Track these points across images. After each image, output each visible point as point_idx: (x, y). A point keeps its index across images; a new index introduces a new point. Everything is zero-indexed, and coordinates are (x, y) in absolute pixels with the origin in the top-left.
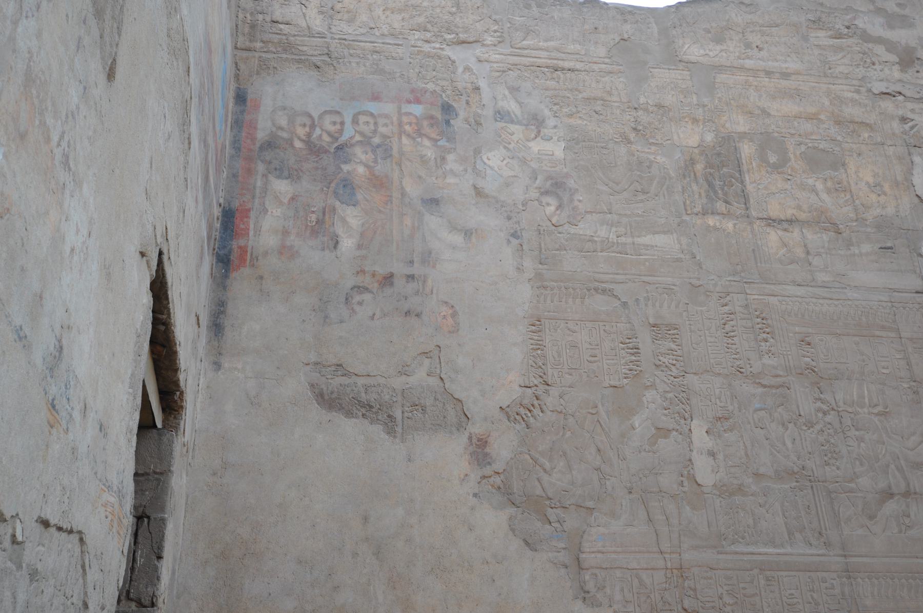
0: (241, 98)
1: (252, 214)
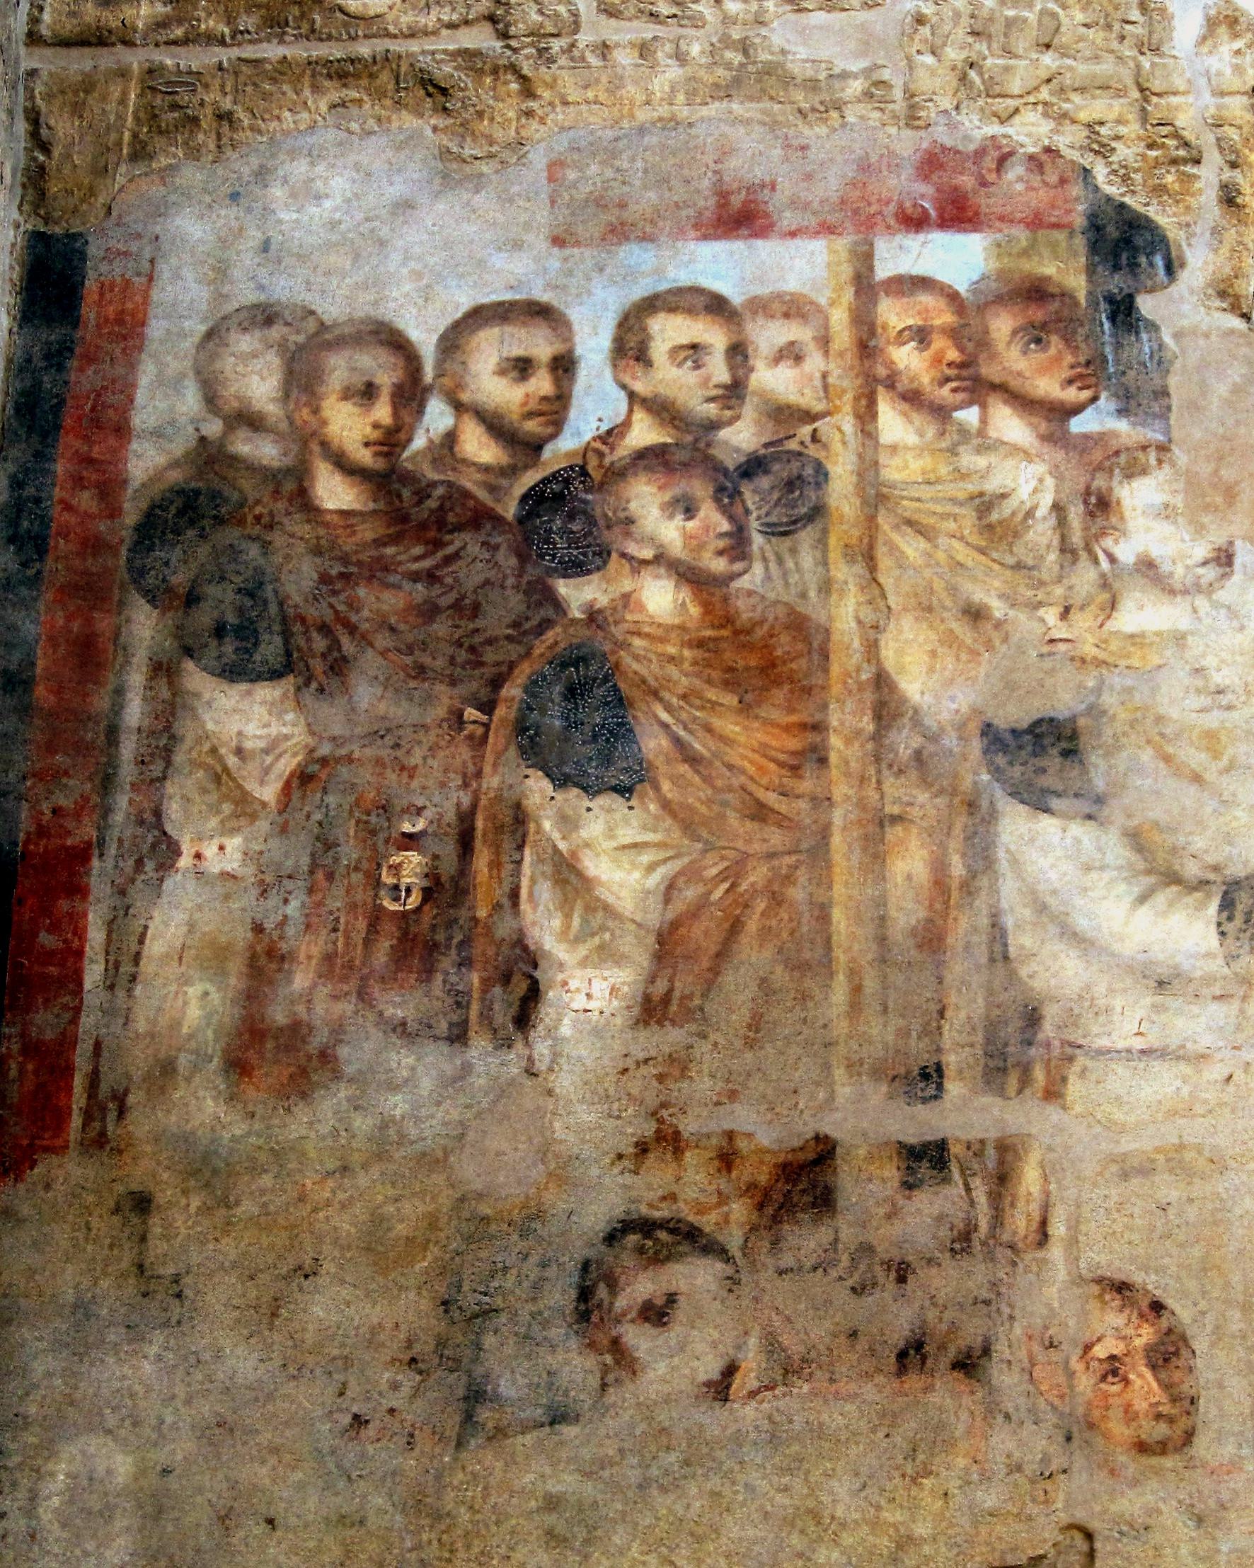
1: (100, 875)
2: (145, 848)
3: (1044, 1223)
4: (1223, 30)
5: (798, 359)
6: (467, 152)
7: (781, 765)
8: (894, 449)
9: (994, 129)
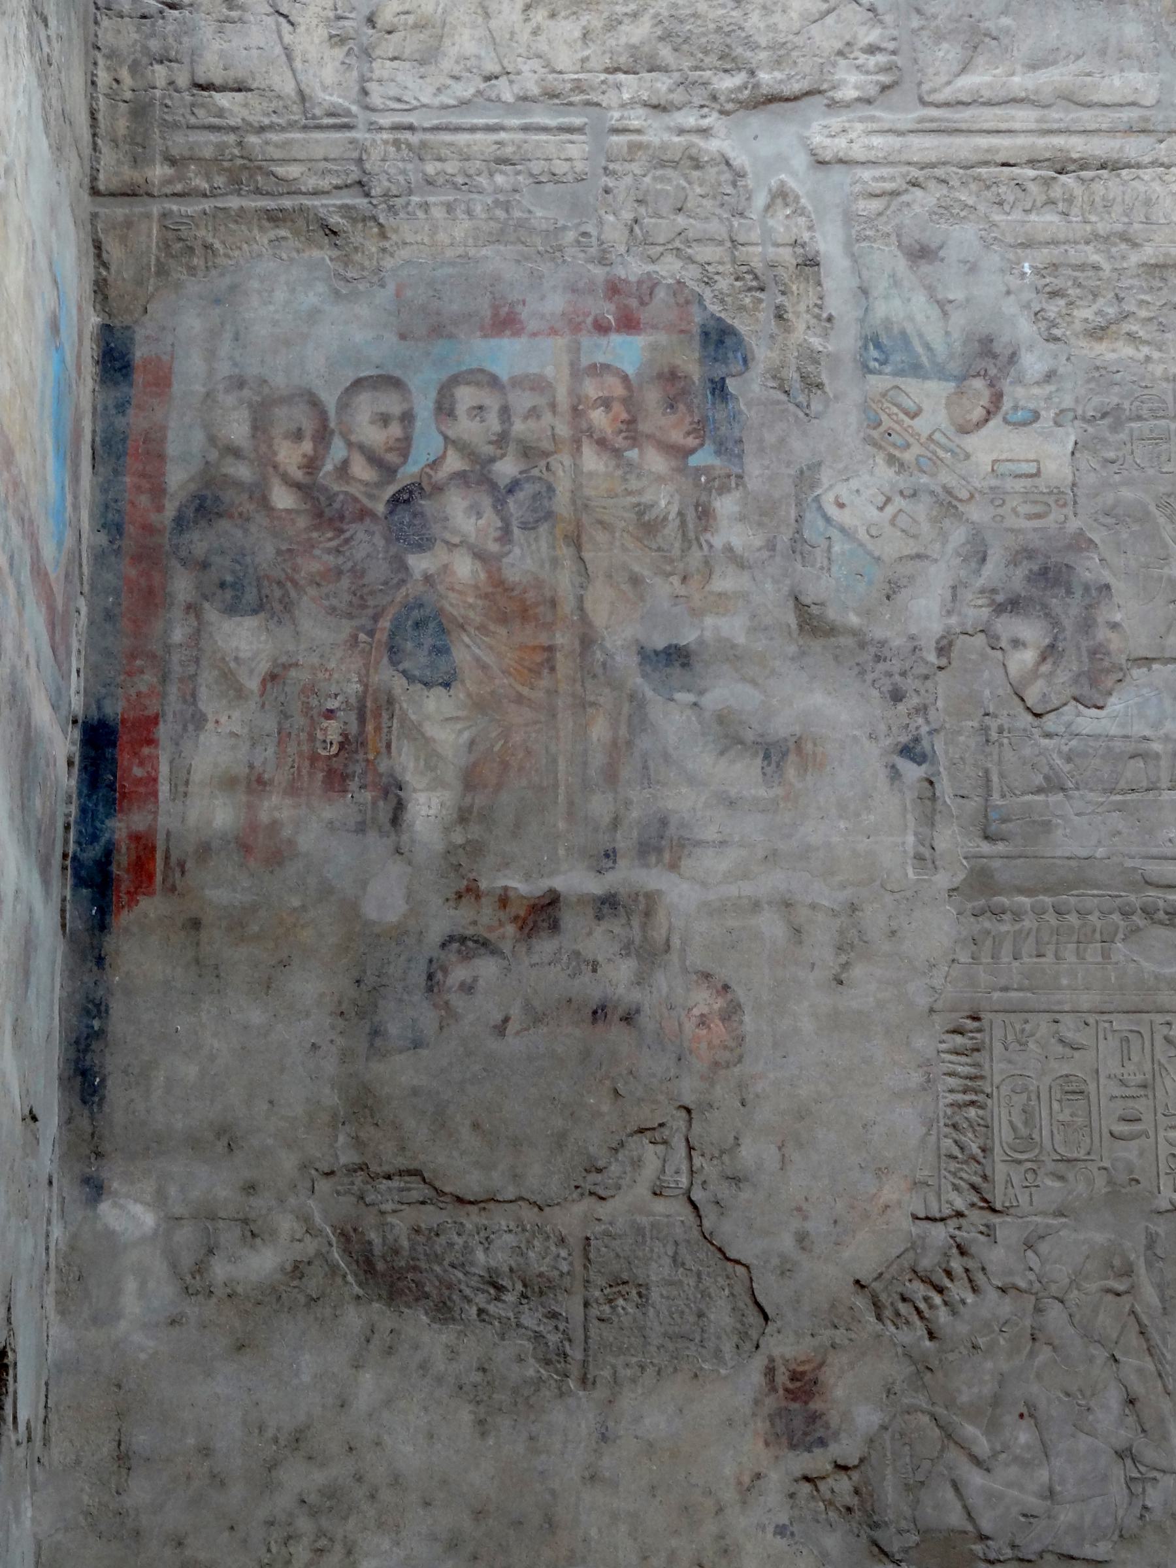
0: (114, 360)
1: (163, 731)
2: (188, 716)
3: (668, 940)
4: (779, 201)
5: (539, 417)
6: (349, 275)
7: (530, 670)
8: (591, 475)
9: (650, 268)
